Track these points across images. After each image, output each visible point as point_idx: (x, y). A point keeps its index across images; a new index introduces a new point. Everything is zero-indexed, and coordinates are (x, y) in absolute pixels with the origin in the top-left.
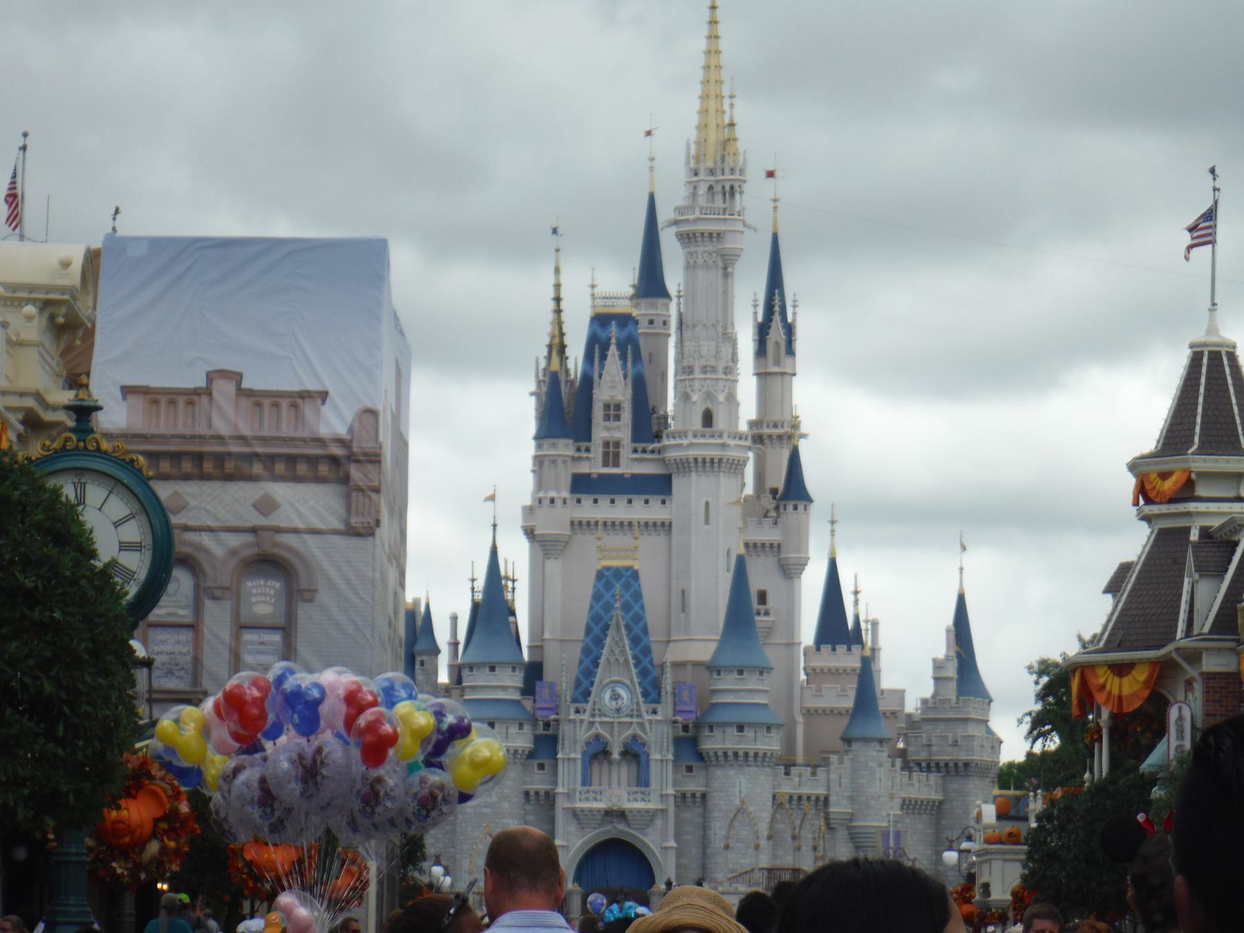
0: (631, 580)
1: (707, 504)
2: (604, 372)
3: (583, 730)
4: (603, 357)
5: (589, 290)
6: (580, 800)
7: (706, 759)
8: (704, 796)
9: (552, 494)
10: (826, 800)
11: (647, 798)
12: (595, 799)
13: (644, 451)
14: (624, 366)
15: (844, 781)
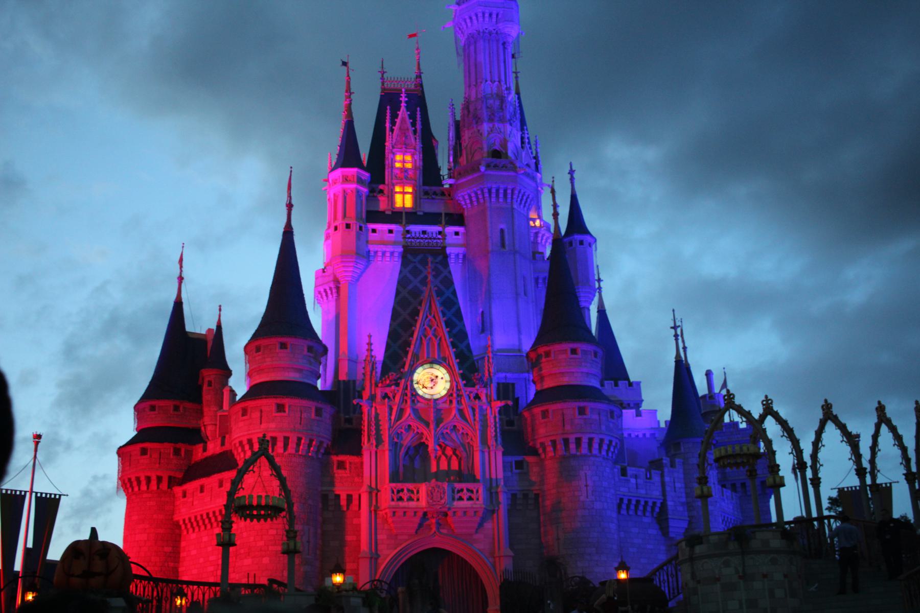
0: (439, 266)
1: (502, 231)
2: (396, 128)
3: (393, 417)
4: (394, 116)
5: (380, 75)
6: (393, 500)
7: (540, 451)
8: (537, 496)
9: (347, 221)
10: (664, 504)
11: (474, 496)
12: (410, 499)
13: (435, 193)
14: (414, 124)
15: (678, 485)
